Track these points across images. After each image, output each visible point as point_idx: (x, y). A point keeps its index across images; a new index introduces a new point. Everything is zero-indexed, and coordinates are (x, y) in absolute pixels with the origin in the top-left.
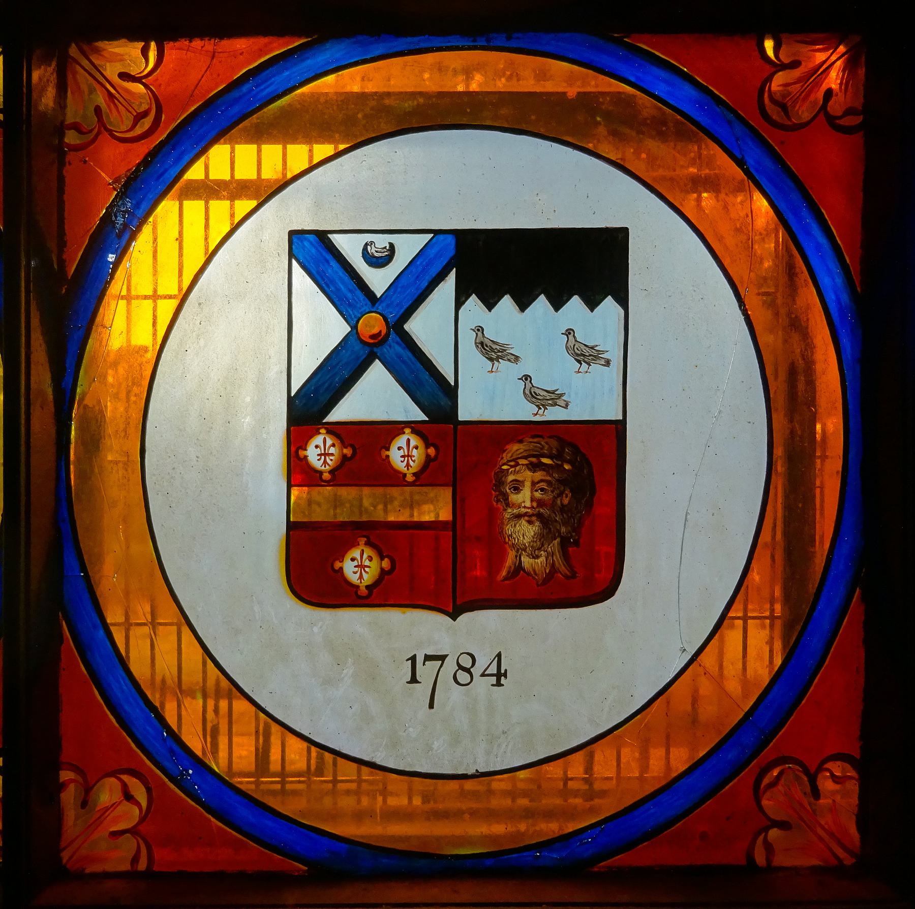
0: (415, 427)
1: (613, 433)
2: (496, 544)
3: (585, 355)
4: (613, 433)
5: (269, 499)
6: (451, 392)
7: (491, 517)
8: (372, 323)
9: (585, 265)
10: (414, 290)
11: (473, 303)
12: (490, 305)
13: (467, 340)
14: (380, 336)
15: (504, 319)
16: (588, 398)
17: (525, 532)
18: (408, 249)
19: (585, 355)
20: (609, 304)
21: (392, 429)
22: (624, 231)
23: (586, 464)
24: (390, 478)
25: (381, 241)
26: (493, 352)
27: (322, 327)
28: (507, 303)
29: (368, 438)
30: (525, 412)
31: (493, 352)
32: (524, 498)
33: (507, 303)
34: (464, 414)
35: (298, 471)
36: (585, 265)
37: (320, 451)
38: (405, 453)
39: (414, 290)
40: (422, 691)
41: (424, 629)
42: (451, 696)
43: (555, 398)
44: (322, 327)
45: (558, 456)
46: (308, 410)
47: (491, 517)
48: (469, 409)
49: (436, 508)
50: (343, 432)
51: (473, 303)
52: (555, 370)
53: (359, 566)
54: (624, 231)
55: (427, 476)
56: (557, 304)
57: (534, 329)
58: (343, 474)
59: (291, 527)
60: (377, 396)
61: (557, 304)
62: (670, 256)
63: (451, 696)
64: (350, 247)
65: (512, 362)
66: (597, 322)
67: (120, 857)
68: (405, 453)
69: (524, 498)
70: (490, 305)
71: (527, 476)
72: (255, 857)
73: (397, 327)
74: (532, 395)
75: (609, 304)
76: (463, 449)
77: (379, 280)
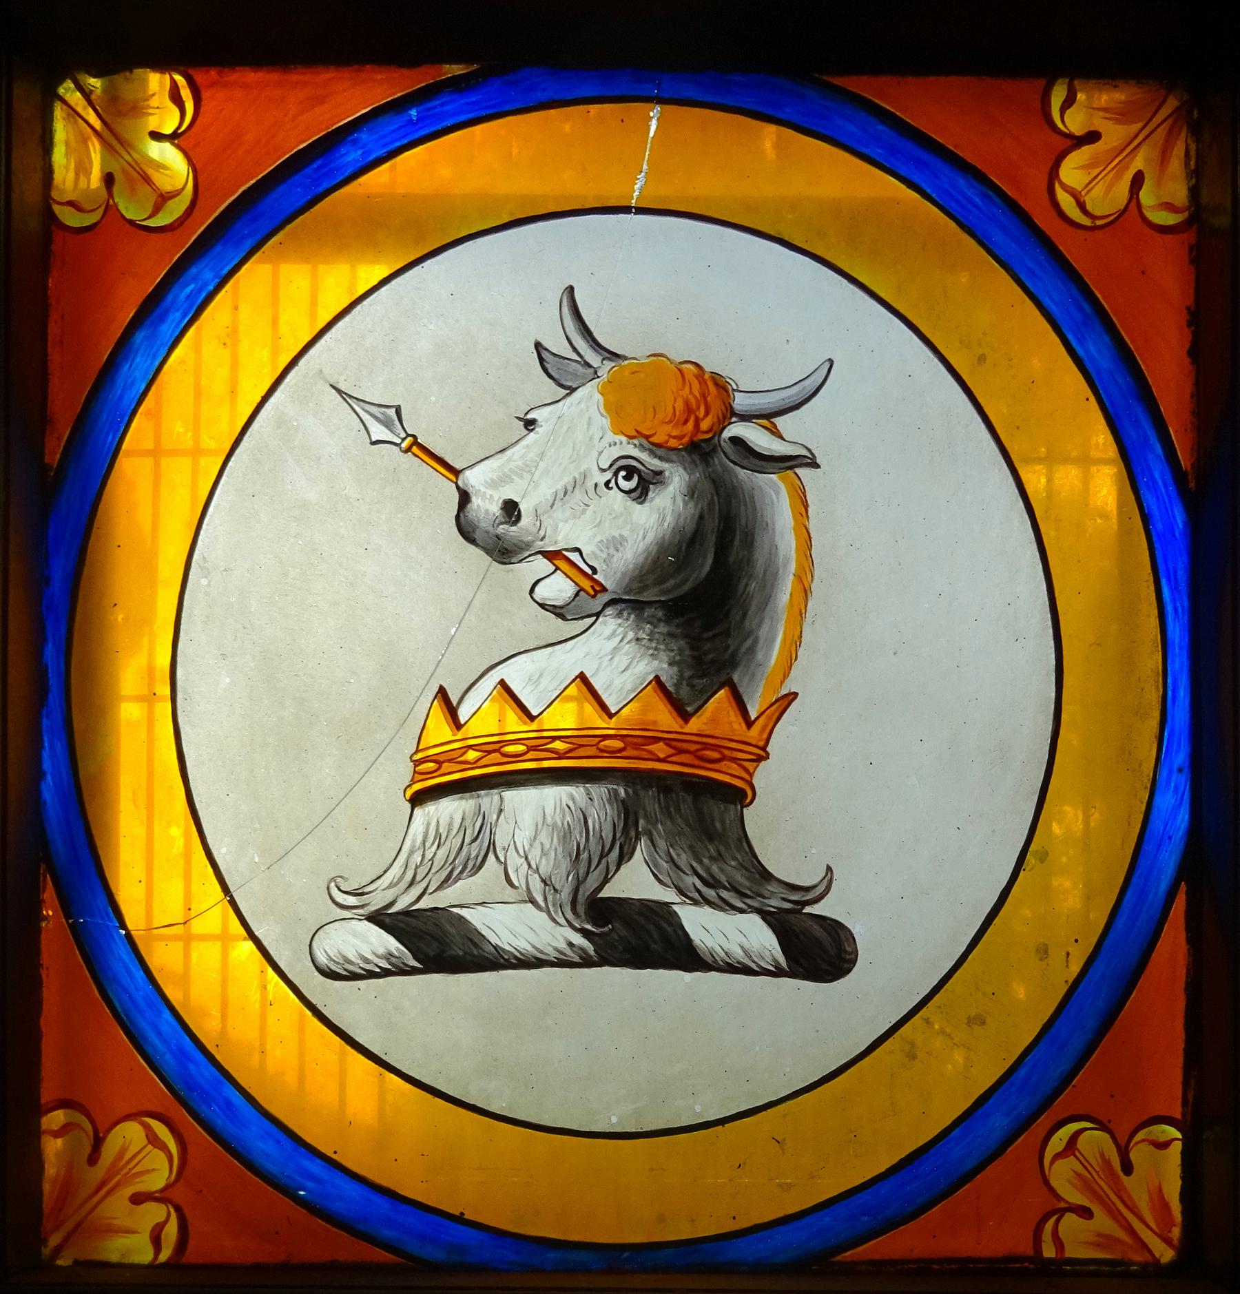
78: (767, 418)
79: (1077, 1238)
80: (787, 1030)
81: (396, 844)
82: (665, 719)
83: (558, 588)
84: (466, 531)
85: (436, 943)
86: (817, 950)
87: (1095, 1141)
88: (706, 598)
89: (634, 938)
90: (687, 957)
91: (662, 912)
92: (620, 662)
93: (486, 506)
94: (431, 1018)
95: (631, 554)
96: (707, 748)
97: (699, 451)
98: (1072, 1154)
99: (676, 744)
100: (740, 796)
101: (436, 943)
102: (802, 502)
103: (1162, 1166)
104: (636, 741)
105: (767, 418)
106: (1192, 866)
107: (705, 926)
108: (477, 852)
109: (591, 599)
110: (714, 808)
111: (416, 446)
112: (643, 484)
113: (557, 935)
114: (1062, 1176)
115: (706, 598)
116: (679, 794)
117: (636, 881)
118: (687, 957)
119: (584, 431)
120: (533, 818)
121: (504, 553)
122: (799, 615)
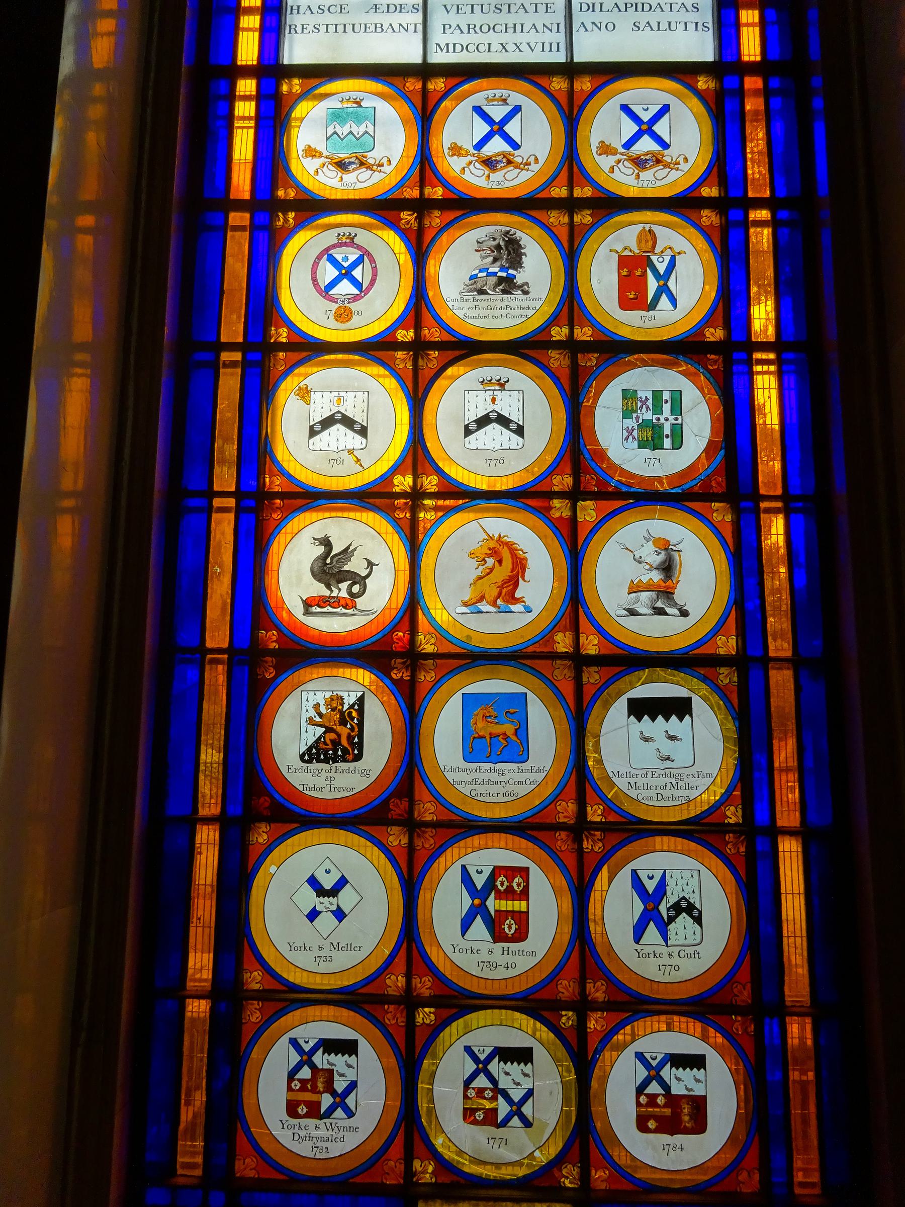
0: (663, 1095)
1: (704, 1098)
2: (680, 1121)
3: (698, 1081)
4: (704, 1098)
5: (632, 1111)
6: (670, 1088)
7: (679, 1115)
8: (653, 1073)
9: (696, 1062)
10: (661, 1065)
11: (674, 1069)
12: (677, 1069)
13: (673, 1076)
14: (654, 1074)
15: (680, 1072)
16: (699, 1091)
17: (686, 1118)
18: (660, 1057)
19: (698, 1081)
20: (702, 1070)
21: (658, 1095)
22: (704, 1055)
23: (699, 1104)
24: (658, 1106)
25: (654, 1055)
26: (679, 1079)
27: (643, 1073)
28: (681, 1069)
29: (652, 1098)
30: (685, 1093)
31: (679, 1079)
32: (686, 1111)
33: (681, 1069)
34: (673, 1093)
35: (639, 1104)
36: (696, 1062)
37: (643, 1099)
38: (661, 1100)
39: (661, 1065)
40: (666, 1151)
41: (665, 1138)
42: (672, 1153)
43: (691, 1090)
44: (643, 1073)
45: (693, 1103)
46: (640, 1090)
47: (679, 1115)
48: (674, 1091)
49: (668, 1111)
50: (647, 1095)
51: (674, 1069)
52: (692, 1084)
53: (652, 1124)
54: (704, 1055)
55: (665, 1106)
56: (692, 1069)
57: (688, 1075)
58: (648, 1105)
59: (637, 1116)
60: (654, 1088)
61: (692, 1069)
62: (714, 1059)
63: (672, 1153)
64: (648, 1056)
65: (682, 1082)
66: (700, 1074)
67: (603, 1186)
68: (661, 1100)
69: (686, 1111)
70: (677, 1069)
71: (686, 1106)
72: (630, 1187)
73: (658, 1073)
74: (687, 1089)
75: (702, 1070)
76: (673, 1100)
77: (654, 1063)
78: (675, 545)
79: (722, 651)
80: (682, 624)
81: (627, 600)
82: (662, 583)
83: (648, 567)
84: (635, 560)
85: (632, 613)
86: (684, 613)
87: (723, 638)
88: (668, 568)
89: (660, 612)
90: (666, 614)
91: (663, 608)
92: (656, 577)
93: (637, 557)
94: (631, 623)
95: (657, 562)
96: (668, 587)
97: (666, 549)
98: (721, 640)
99: (664, 587)
100: (673, 594)
101: (632, 613)
102: (680, 556)
103: (733, 641)
104: (659, 587)
105: (675, 545)
106: (735, 602)
107: (668, 610)
108: (637, 600)
109: (652, 568)
110: (670, 596)
111: (627, 549)
112: (659, 554)
113: (650, 611)
114: (719, 643)
115: (668, 568)
116: (667, 594)
117: (659, 604)
118: (666, 614)
119: (650, 547)
120: (645, 596)
121: (640, 562)
122: (680, 570)
